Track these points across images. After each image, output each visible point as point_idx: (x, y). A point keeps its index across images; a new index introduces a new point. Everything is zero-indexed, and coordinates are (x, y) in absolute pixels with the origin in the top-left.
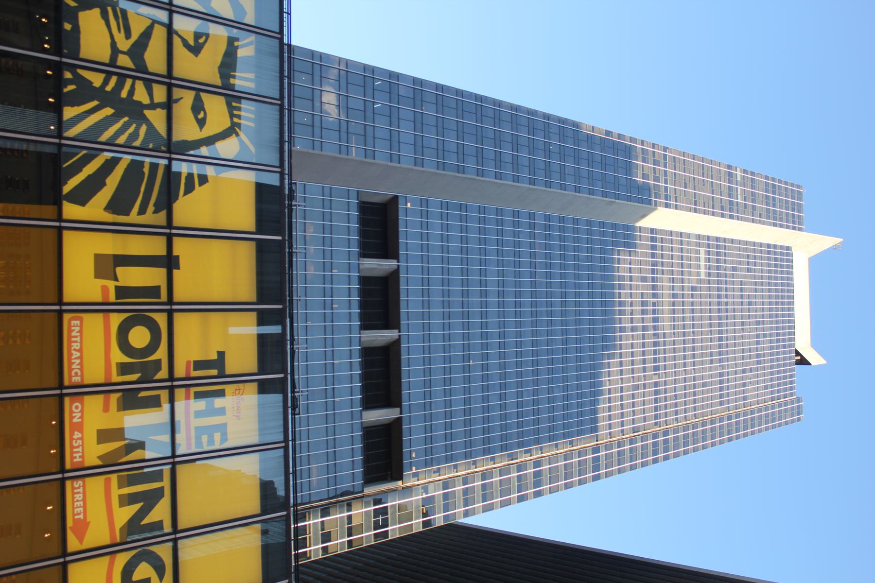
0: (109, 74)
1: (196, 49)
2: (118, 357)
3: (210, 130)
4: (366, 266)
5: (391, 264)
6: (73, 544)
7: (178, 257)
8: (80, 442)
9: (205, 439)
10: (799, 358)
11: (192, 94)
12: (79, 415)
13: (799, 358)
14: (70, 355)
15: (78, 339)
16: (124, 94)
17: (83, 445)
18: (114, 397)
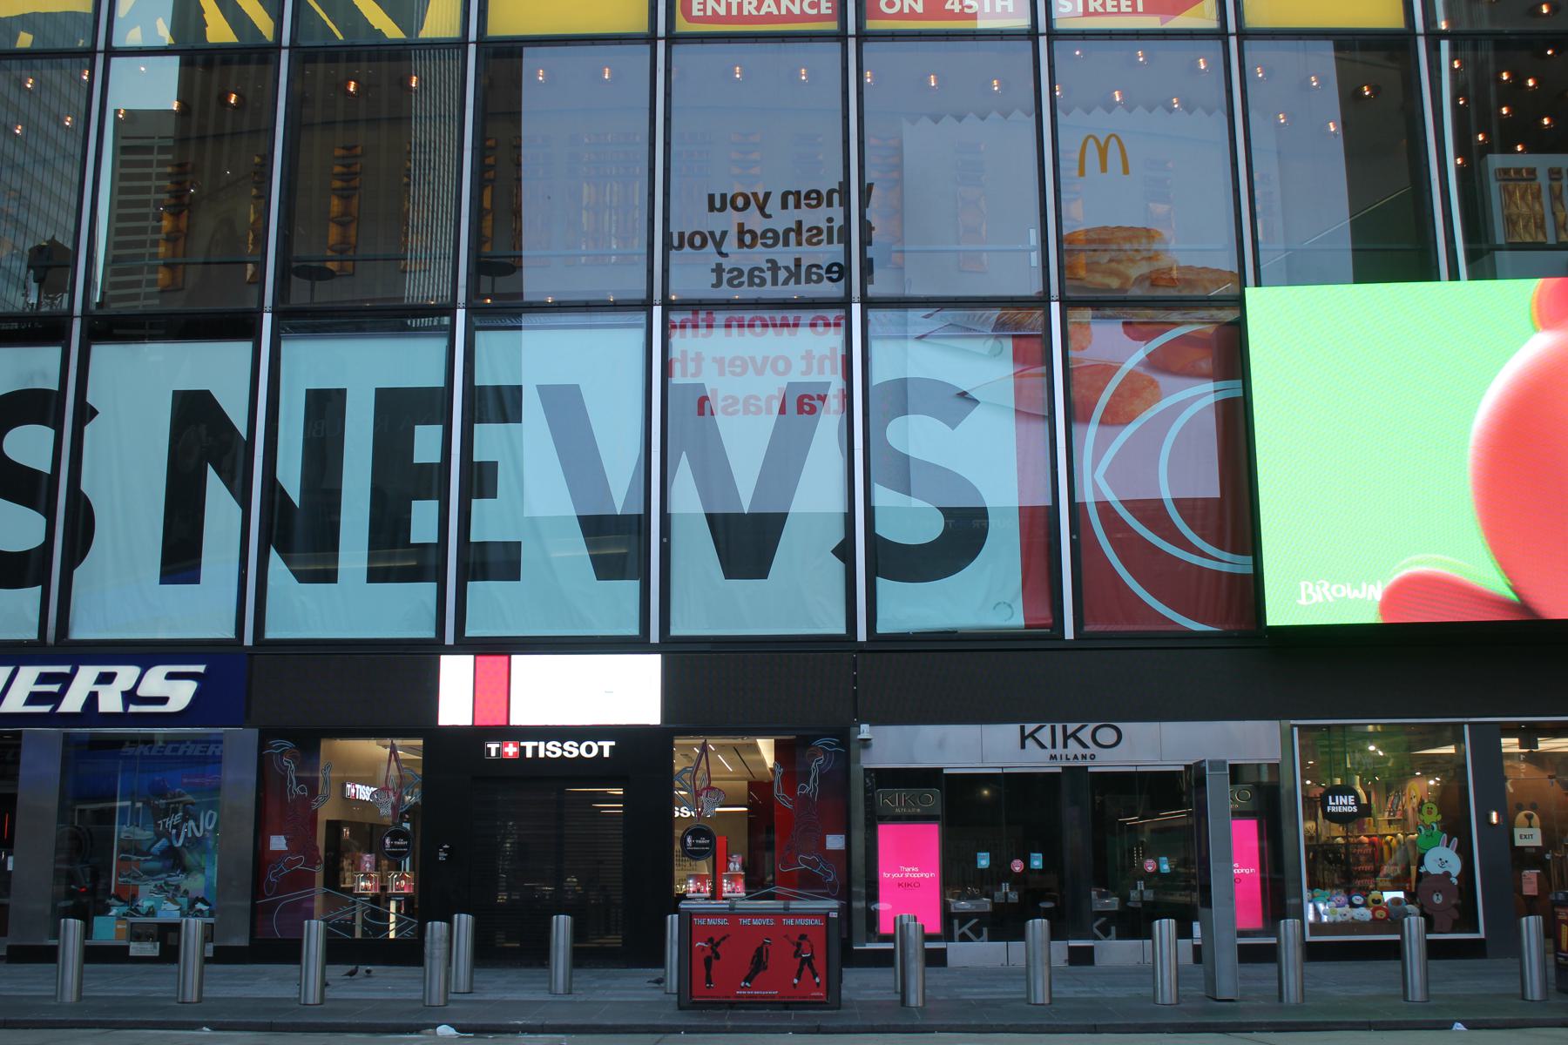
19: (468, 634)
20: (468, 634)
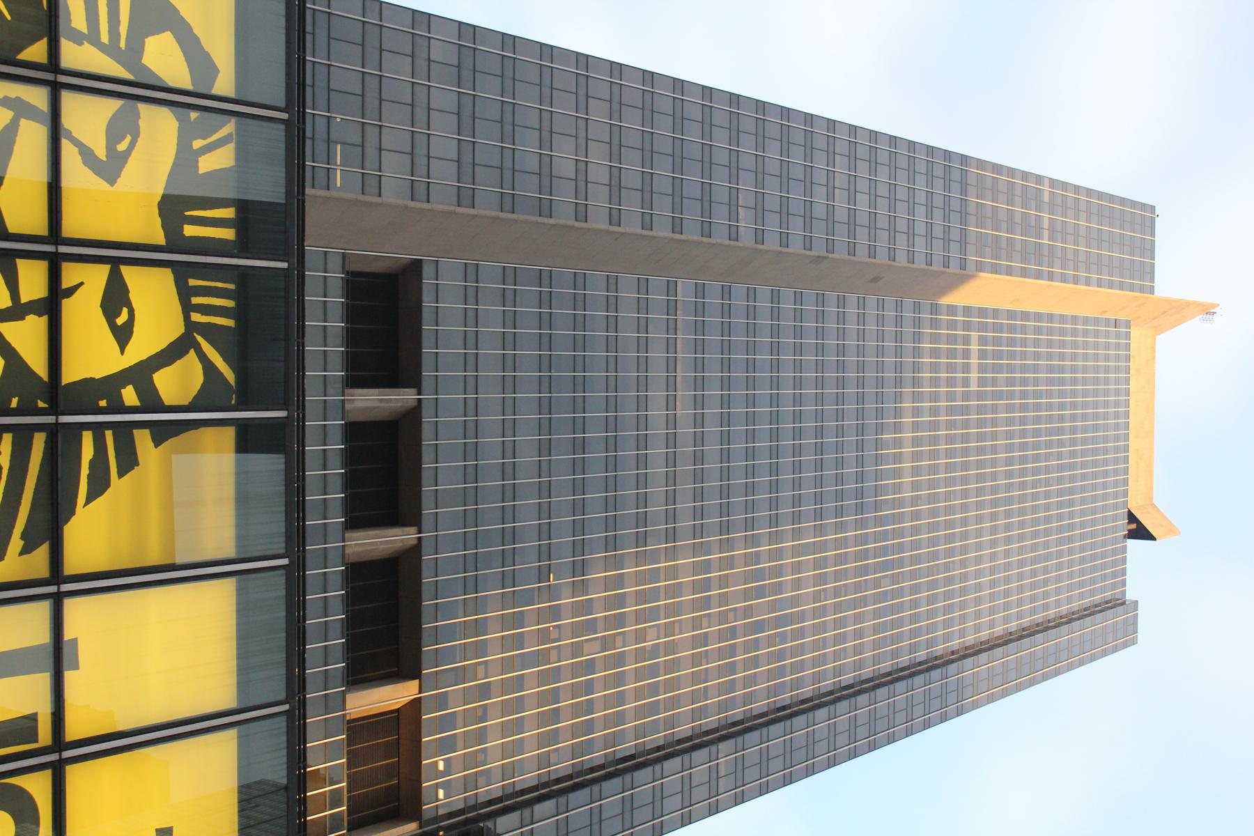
3: (143, 346)
4: (359, 405)
5: (406, 397)
7: (75, 641)
10: (1134, 526)
11: (103, 271)
13: (1134, 526)
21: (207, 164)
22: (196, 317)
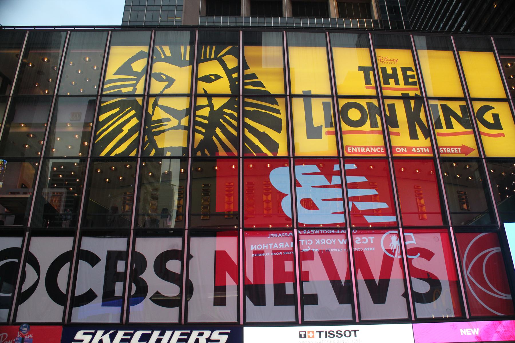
0: (195, 130)
1: (171, 81)
2: (367, 127)
3: (221, 72)
6: (474, 154)
8: (418, 149)
9: (411, 80)
12: (402, 149)
14: (368, 153)
15: (359, 148)
16: (206, 122)
17: (420, 147)
18: (391, 130)
19: (305, 320)
20: (305, 320)
21: (168, 54)
22: (213, 57)
